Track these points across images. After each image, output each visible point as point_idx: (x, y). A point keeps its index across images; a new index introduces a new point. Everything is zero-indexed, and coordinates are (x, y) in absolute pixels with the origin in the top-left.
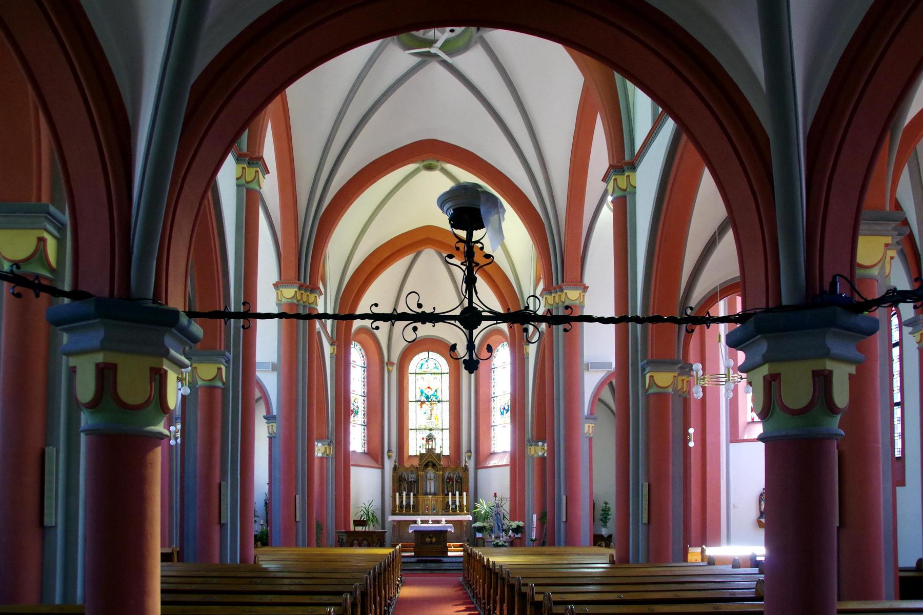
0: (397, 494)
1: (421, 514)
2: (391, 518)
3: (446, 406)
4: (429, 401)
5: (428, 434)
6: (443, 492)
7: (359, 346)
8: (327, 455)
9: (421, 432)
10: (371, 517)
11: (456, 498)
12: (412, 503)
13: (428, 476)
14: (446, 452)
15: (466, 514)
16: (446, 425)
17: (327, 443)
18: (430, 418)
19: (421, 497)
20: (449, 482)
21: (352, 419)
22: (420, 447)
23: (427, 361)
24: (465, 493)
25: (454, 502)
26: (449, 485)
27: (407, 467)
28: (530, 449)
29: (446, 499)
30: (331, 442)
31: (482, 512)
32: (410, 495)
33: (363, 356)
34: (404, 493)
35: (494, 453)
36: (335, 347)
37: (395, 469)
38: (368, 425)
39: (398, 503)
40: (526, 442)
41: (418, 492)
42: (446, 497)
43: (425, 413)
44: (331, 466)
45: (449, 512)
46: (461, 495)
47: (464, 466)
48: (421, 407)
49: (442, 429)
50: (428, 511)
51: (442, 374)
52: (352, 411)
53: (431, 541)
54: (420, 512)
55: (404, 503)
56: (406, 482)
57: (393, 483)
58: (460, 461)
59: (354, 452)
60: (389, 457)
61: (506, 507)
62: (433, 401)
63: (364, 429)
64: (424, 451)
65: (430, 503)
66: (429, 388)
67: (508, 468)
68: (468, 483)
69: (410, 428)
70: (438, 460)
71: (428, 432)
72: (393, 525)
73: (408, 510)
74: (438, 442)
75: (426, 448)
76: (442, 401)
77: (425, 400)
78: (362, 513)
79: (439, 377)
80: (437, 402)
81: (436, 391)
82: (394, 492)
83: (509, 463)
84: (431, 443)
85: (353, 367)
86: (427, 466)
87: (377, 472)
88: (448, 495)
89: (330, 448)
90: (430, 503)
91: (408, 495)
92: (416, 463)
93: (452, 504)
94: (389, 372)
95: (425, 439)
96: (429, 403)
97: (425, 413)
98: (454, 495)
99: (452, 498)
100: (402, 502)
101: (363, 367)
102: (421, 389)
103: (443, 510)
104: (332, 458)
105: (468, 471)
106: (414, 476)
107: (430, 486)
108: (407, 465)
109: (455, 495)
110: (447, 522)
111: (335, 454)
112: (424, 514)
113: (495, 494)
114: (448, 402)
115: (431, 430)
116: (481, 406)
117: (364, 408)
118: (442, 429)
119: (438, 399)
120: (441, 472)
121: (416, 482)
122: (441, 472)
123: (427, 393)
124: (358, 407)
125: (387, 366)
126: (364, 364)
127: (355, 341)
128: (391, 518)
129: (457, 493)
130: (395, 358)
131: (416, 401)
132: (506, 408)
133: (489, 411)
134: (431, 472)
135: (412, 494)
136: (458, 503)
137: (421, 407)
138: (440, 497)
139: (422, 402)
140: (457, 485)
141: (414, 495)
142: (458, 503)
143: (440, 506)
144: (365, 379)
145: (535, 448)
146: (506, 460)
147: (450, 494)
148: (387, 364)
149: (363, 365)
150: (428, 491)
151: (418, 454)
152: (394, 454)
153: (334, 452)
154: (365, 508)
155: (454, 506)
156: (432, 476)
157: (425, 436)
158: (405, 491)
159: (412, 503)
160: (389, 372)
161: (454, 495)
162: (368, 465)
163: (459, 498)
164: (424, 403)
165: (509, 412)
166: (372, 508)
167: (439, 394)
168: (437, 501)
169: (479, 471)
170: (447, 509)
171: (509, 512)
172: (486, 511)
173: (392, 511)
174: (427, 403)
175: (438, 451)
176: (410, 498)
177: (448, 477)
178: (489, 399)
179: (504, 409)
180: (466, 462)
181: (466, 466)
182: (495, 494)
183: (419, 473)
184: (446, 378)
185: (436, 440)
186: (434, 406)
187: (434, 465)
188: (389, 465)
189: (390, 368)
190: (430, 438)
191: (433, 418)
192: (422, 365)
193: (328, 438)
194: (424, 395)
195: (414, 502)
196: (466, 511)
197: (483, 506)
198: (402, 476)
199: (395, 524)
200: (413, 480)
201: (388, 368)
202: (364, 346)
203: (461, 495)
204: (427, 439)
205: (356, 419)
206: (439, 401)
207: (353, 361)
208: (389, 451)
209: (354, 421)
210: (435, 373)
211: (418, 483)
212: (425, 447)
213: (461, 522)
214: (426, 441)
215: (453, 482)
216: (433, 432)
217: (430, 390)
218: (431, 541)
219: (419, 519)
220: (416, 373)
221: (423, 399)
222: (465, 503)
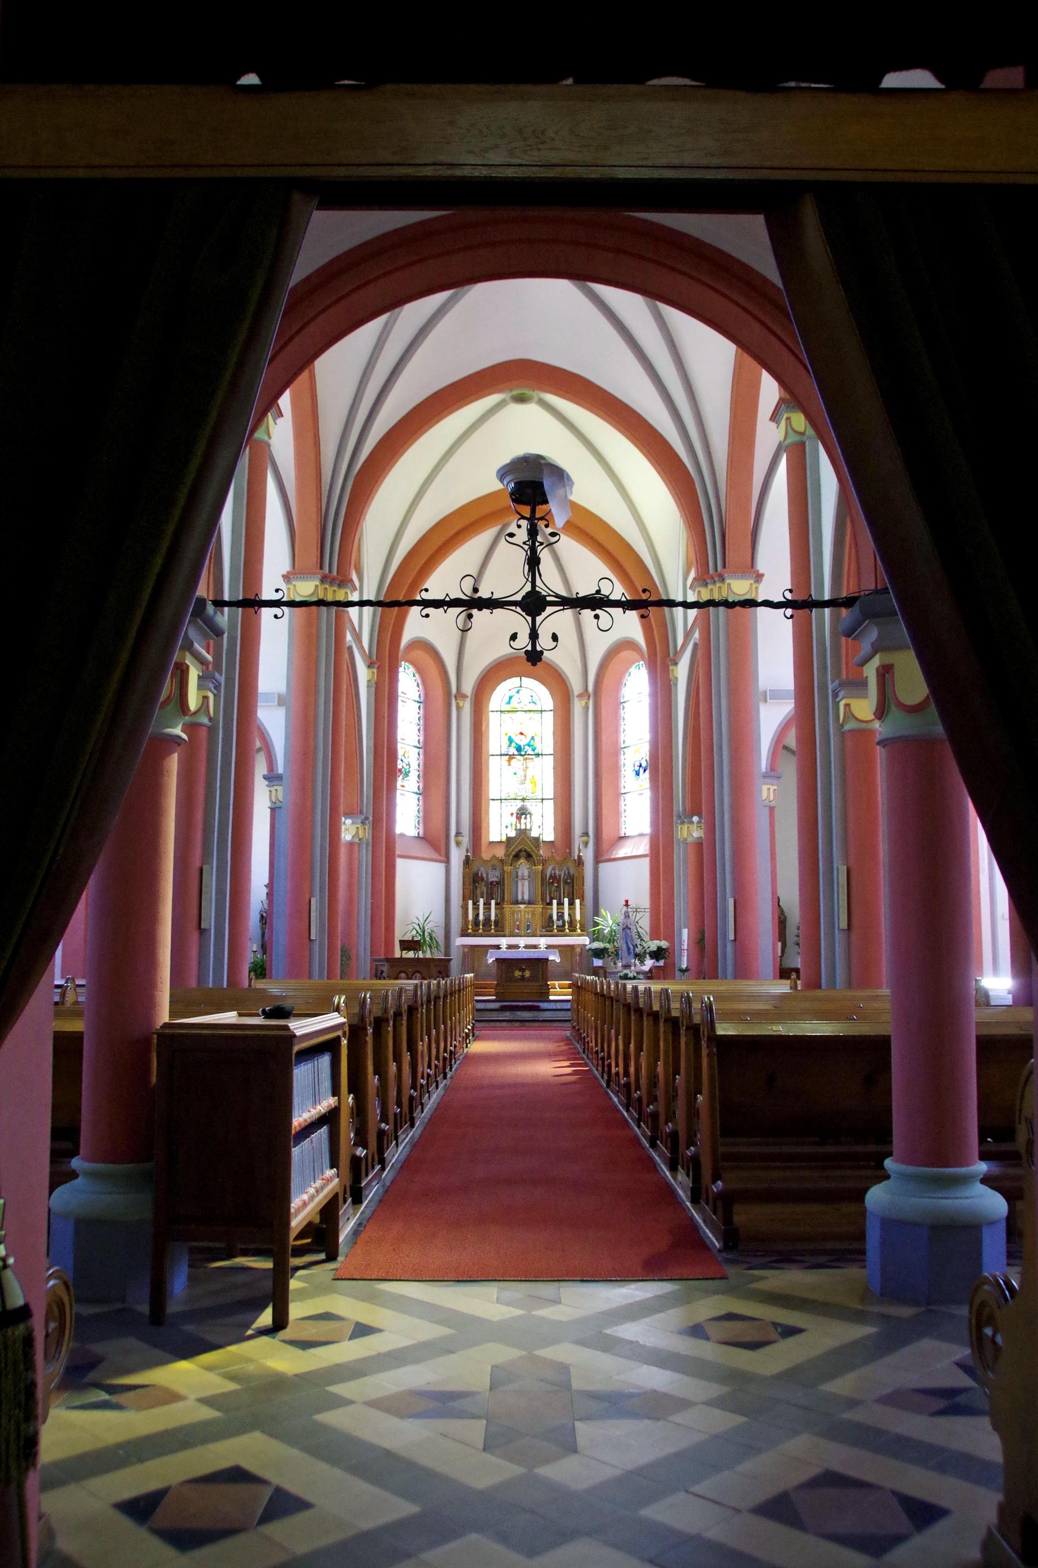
0: (470, 902)
1: (507, 934)
2: (460, 941)
3: (548, 762)
4: (521, 755)
5: (519, 806)
6: (543, 899)
7: (411, 670)
8: (360, 839)
9: (509, 804)
10: (428, 939)
11: (563, 909)
12: (493, 918)
13: (520, 874)
14: (549, 835)
15: (579, 935)
16: (549, 792)
17: (359, 821)
18: (523, 783)
19: (507, 908)
21: (400, 782)
22: (507, 827)
23: (518, 692)
24: (578, 902)
25: (561, 916)
26: (553, 888)
27: (486, 859)
28: (681, 828)
29: (549, 911)
30: (367, 818)
31: (606, 932)
32: (490, 904)
33: (418, 685)
35: (625, 837)
36: (375, 671)
37: (467, 862)
38: (425, 793)
39: (471, 917)
40: (675, 818)
42: (549, 907)
43: (515, 774)
44: (365, 857)
46: (572, 903)
47: (576, 858)
48: (509, 765)
49: (543, 799)
50: (518, 929)
51: (541, 711)
52: (400, 770)
53: (523, 976)
54: (507, 931)
55: (481, 917)
56: (484, 883)
57: (464, 885)
59: (402, 835)
60: (458, 844)
61: (644, 923)
63: (418, 799)
64: (512, 834)
65: (523, 917)
66: (522, 734)
67: (647, 860)
68: (583, 885)
69: (491, 798)
70: (536, 847)
71: (519, 804)
72: (464, 952)
74: (536, 819)
75: (516, 829)
76: (542, 755)
77: (516, 753)
78: (414, 932)
79: (538, 715)
80: (534, 756)
81: (533, 738)
82: (465, 899)
83: (647, 852)
84: (523, 821)
85: (402, 701)
86: (517, 856)
87: (438, 868)
88: (551, 904)
89: (365, 829)
90: (523, 917)
91: (487, 904)
92: (500, 853)
93: (558, 920)
94: (458, 708)
95: (515, 815)
97: (515, 774)
98: (560, 904)
99: (557, 909)
100: (478, 915)
101: (418, 702)
102: (508, 735)
103: (543, 927)
104: (367, 844)
105: (583, 866)
106: (497, 873)
107: (523, 890)
108: (486, 855)
109: (563, 904)
110: (549, 947)
111: (373, 838)
112: (512, 935)
113: (627, 901)
114: (552, 756)
115: (523, 800)
116: (605, 763)
117: (419, 765)
118: (543, 799)
119: (536, 751)
120: (540, 867)
121: (500, 883)
122: (540, 867)
123: (519, 743)
124: (409, 765)
125: (456, 699)
126: (420, 696)
127: (406, 661)
128: (460, 941)
129: (566, 900)
130: (468, 688)
131: (501, 755)
132: (644, 764)
133: (616, 769)
134: (523, 868)
135: (493, 902)
136: (566, 917)
137: (509, 765)
138: (539, 908)
139: (511, 757)
140: (566, 888)
141: (497, 904)
142: (566, 917)
143: (538, 922)
144: (421, 721)
145: (688, 827)
146: (643, 847)
147: (555, 902)
148: (455, 697)
149: (417, 699)
150: (520, 897)
151: (504, 839)
152: (466, 840)
153: (371, 837)
154: (419, 925)
156: (526, 873)
157: (514, 810)
158: (483, 897)
159: (493, 918)
160: (458, 708)
161: (560, 904)
162: (426, 856)
163: (569, 909)
164: (514, 758)
165: (647, 772)
166: (429, 925)
167: (537, 743)
168: (533, 914)
169: (601, 865)
170: (549, 926)
171: (648, 930)
172: (612, 930)
173: (462, 930)
174: (519, 757)
175: (534, 834)
176: (490, 909)
177: (551, 876)
178: (616, 751)
179: (640, 766)
180: (579, 851)
181: (579, 857)
182: (627, 901)
183: (506, 868)
184: (549, 717)
185: (532, 817)
186: (530, 763)
187: (529, 856)
188: (457, 856)
189: (461, 704)
190: (522, 813)
191: (528, 781)
192: (511, 698)
193: (361, 812)
194: (513, 745)
195: (496, 916)
196: (579, 931)
197: (607, 921)
198: (477, 874)
199: (466, 950)
201: (458, 704)
202: (419, 670)
203: (572, 903)
204: (517, 814)
205: (405, 783)
206: (538, 755)
207: (403, 693)
208: (458, 834)
209: (403, 786)
210: (531, 711)
211: (504, 885)
212: (514, 827)
213: (572, 947)
214: (517, 817)
215: (559, 882)
216: (528, 804)
218: (523, 976)
219: (504, 942)
220: (501, 711)
221: (513, 751)
222: (578, 917)
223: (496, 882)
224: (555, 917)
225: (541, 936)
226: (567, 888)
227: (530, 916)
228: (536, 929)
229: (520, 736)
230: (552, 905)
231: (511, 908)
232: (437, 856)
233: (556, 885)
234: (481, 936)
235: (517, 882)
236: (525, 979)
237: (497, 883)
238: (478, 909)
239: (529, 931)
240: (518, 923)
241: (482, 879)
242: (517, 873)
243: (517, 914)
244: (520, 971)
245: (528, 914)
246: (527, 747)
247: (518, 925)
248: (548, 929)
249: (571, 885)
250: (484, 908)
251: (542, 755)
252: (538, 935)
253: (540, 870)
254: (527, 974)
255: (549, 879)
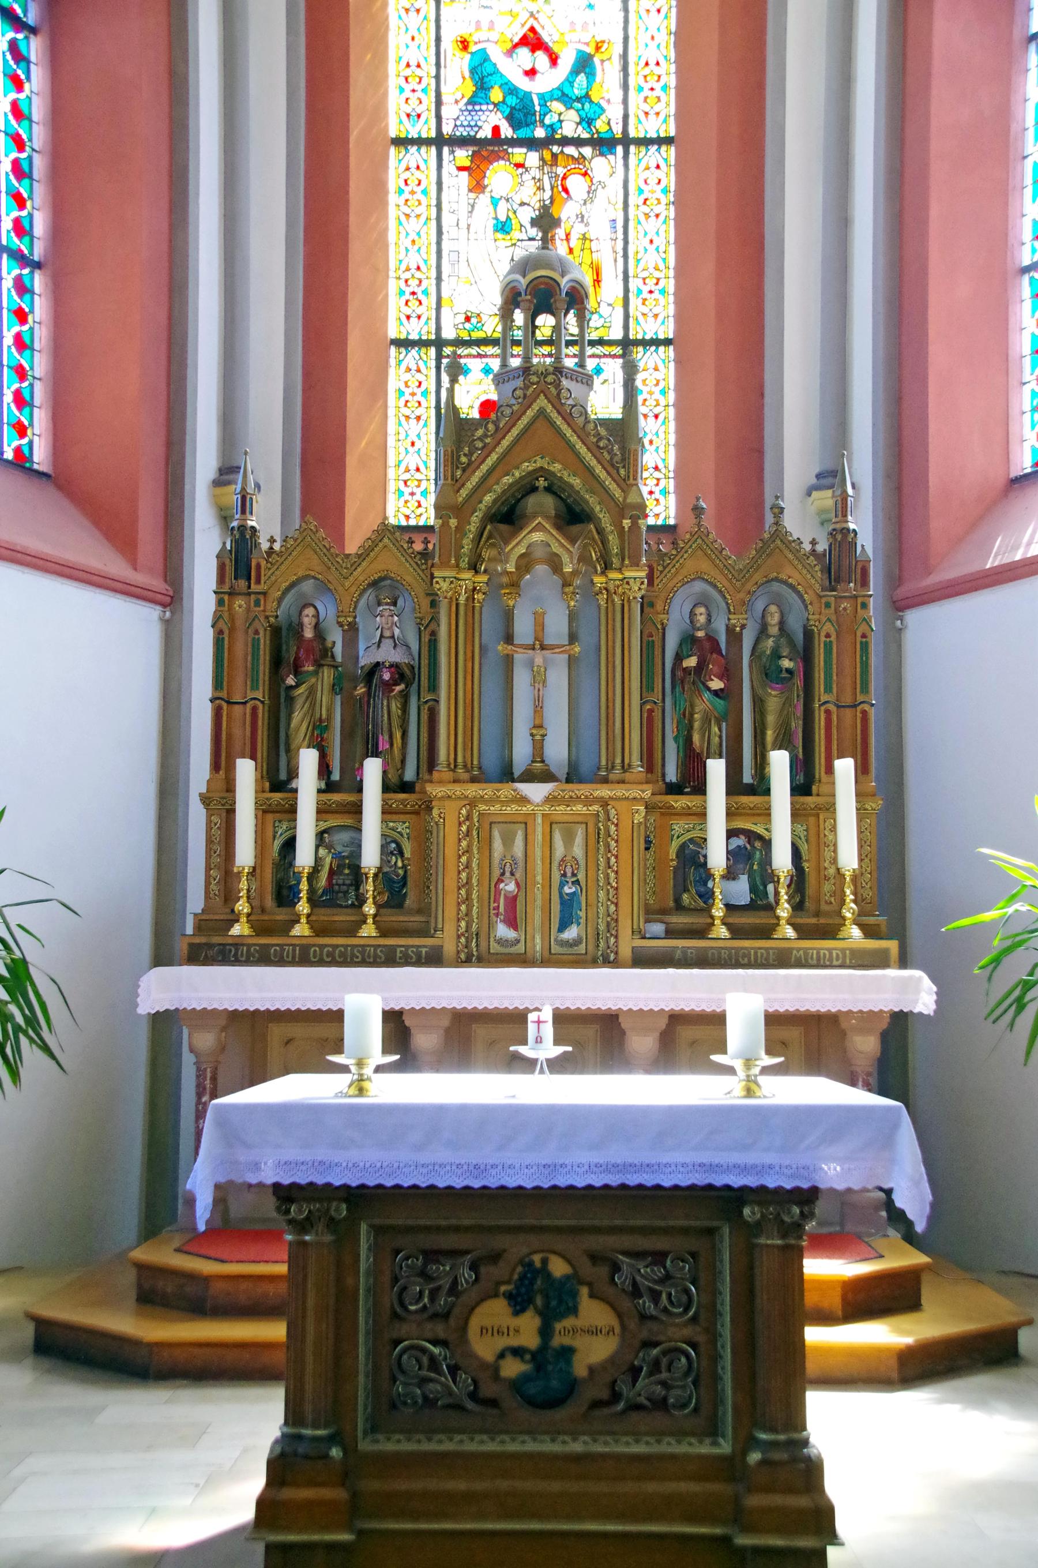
0: (246, 771)
1: (449, 948)
4: (531, 144)
6: (651, 761)
11: (766, 813)
12: (370, 858)
13: (523, 628)
26: (704, 703)
29: (679, 826)
34: (308, 760)
39: (245, 854)
41: (432, 763)
42: (680, 802)
48: (478, 186)
50: (512, 923)
54: (448, 941)
56: (327, 675)
62: (565, 141)
65: (538, 853)
66: (533, 41)
70: (611, 467)
73: (342, 917)
76: (626, 141)
77: (506, 131)
80: (587, 151)
81: (584, 64)
90: (538, 853)
96: (533, 158)
99: (730, 814)
103: (652, 913)
107: (538, 708)
109: (761, 787)
114: (670, 153)
118: (627, 344)
119: (600, 125)
123: (524, 84)
129: (779, 762)
131: (439, 141)
135: (372, 770)
137: (478, 186)
140: (773, 702)
142: (782, 860)
147: (716, 770)
150: (522, 752)
155: (741, 890)
156: (557, 626)
159: (370, 858)
163: (796, 814)
164: (497, 157)
174: (518, 153)
176: (356, 810)
177: (689, 642)
194: (496, 95)
195: (390, 847)
196: (856, 932)
198: (297, 629)
200: (389, 654)
206: (604, 144)
211: (433, 687)
215: (731, 673)
217: (541, 59)
223: (395, 666)
224: (717, 857)
225: (642, 960)
227: (578, 851)
228: (613, 923)
229: (524, 52)
230: (701, 789)
231: (472, 803)
232: (116, 566)
233: (716, 684)
234: (304, 957)
235: (508, 661)
237: (400, 673)
238: (291, 811)
239: (572, 933)
240: (511, 887)
241: (322, 654)
242: (508, 617)
243: (508, 841)
245: (569, 840)
246: (557, 106)
247: (512, 901)
248: (680, 920)
249: (799, 682)
250: (322, 811)
251: (626, 141)
252: (625, 951)
253: (637, 590)
255: (679, 658)
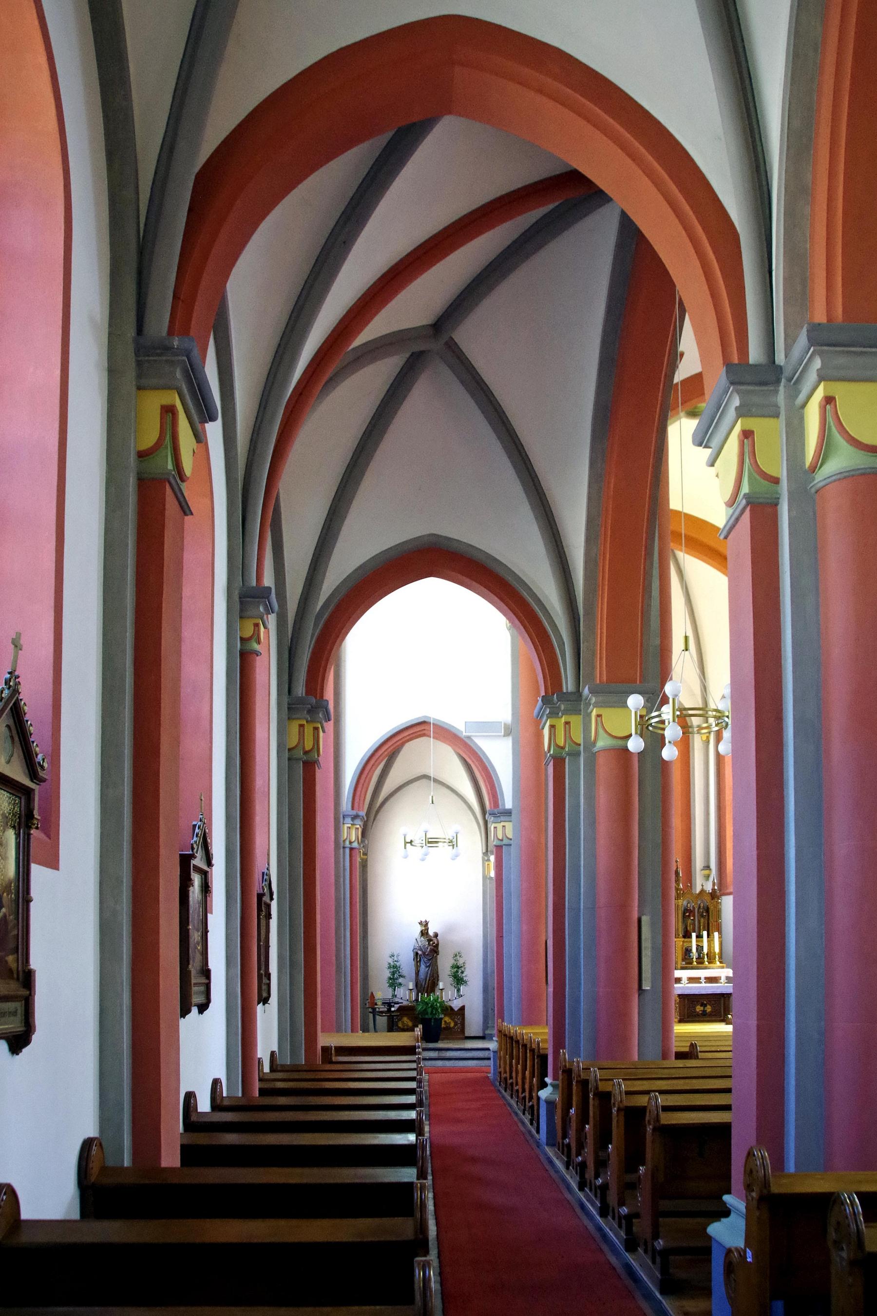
11: (702, 941)
20: (689, 916)
24: (716, 934)
25: (700, 948)
45: (691, 963)
58: (691, 884)
88: (690, 937)
98: (699, 936)
99: (697, 941)
147: (694, 935)
161: (699, 936)
215: (694, 916)
222: (717, 950)
226: (702, 920)
233: (692, 918)
236: (707, 1014)
244: (701, 1006)
254: (709, 1009)
